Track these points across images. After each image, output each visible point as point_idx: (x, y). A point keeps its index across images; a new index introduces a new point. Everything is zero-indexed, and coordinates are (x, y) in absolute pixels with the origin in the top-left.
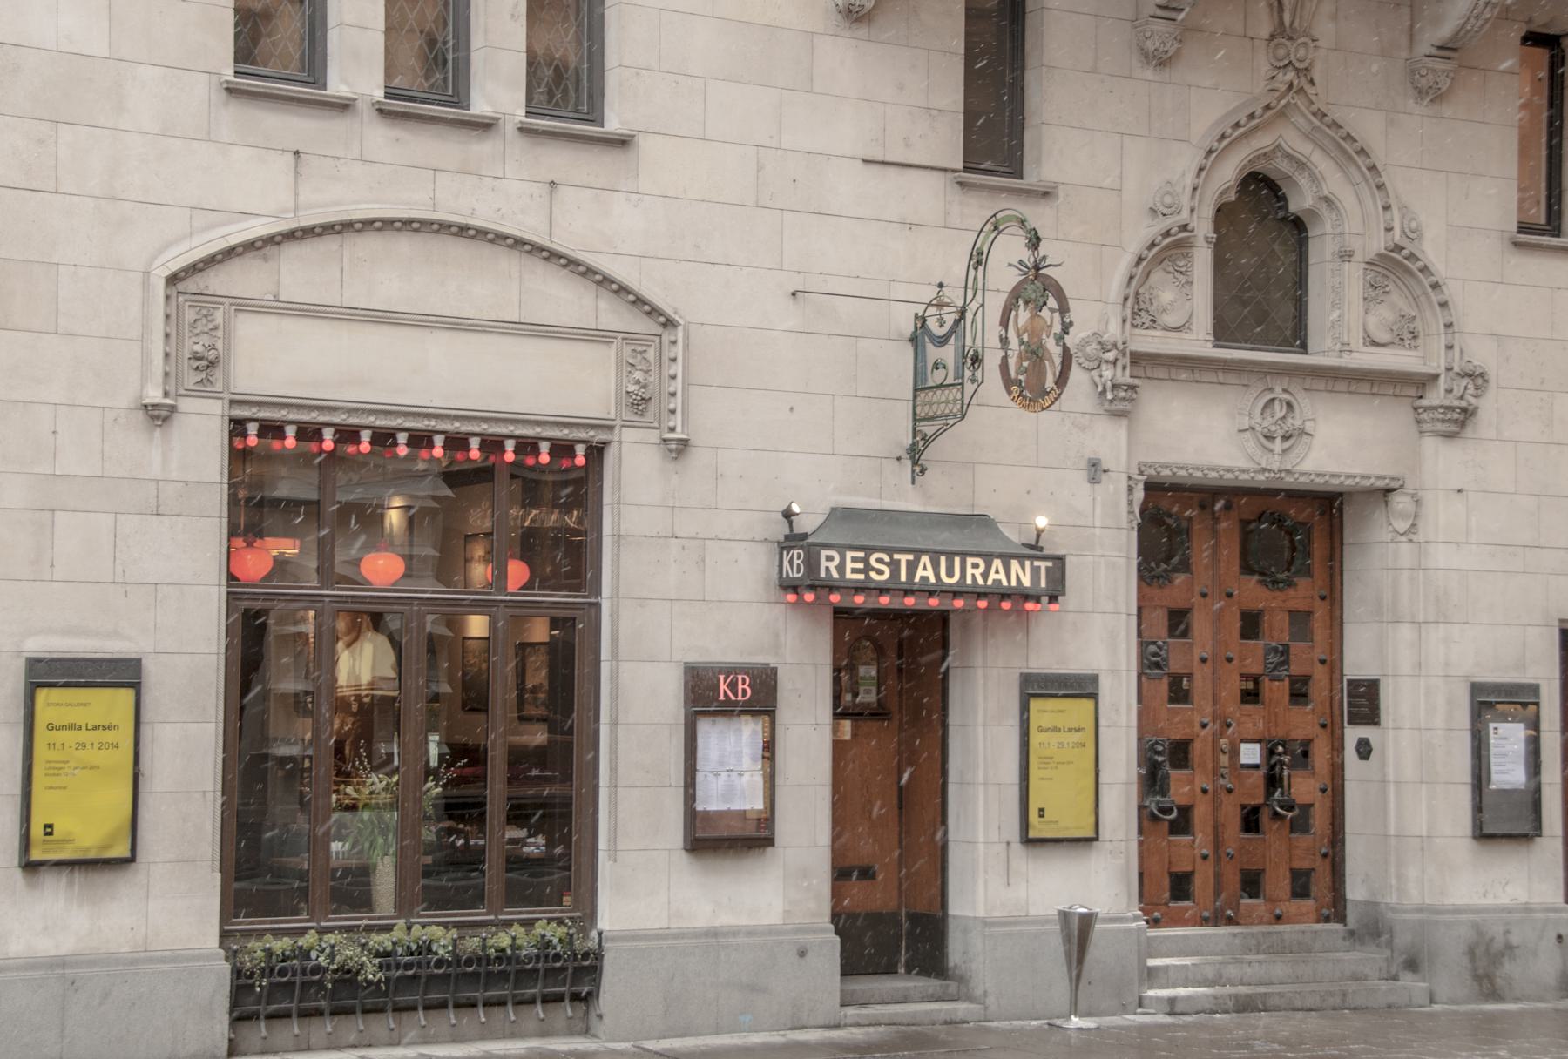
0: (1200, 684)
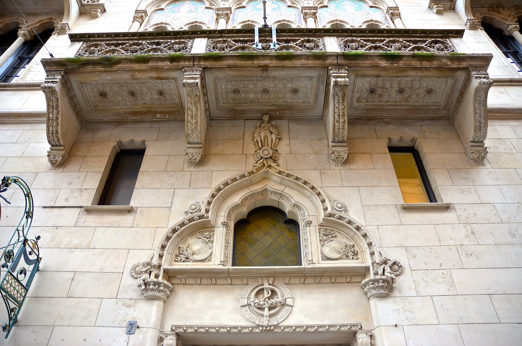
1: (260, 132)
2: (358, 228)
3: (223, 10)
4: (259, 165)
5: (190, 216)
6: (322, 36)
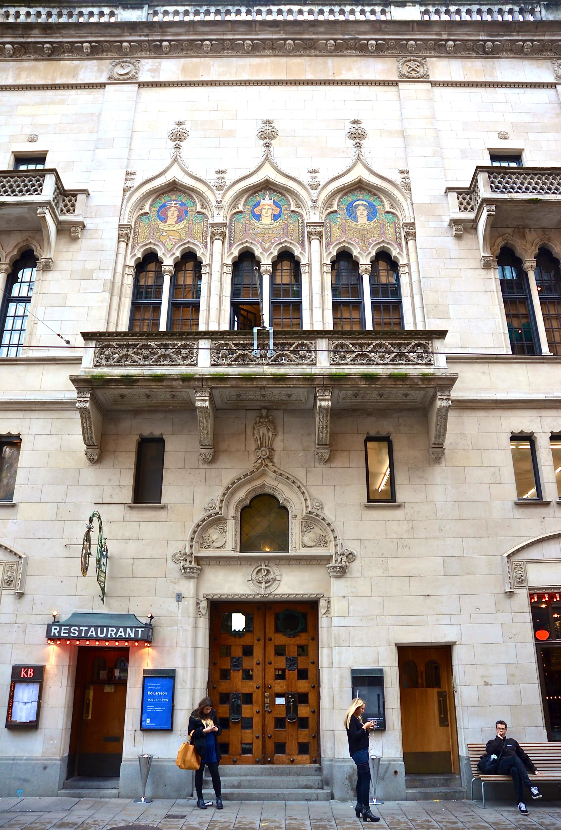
0: (257, 672)
1: (259, 429)
2: (329, 524)
3: (217, 226)
4: (258, 465)
5: (208, 513)
6: (315, 339)
